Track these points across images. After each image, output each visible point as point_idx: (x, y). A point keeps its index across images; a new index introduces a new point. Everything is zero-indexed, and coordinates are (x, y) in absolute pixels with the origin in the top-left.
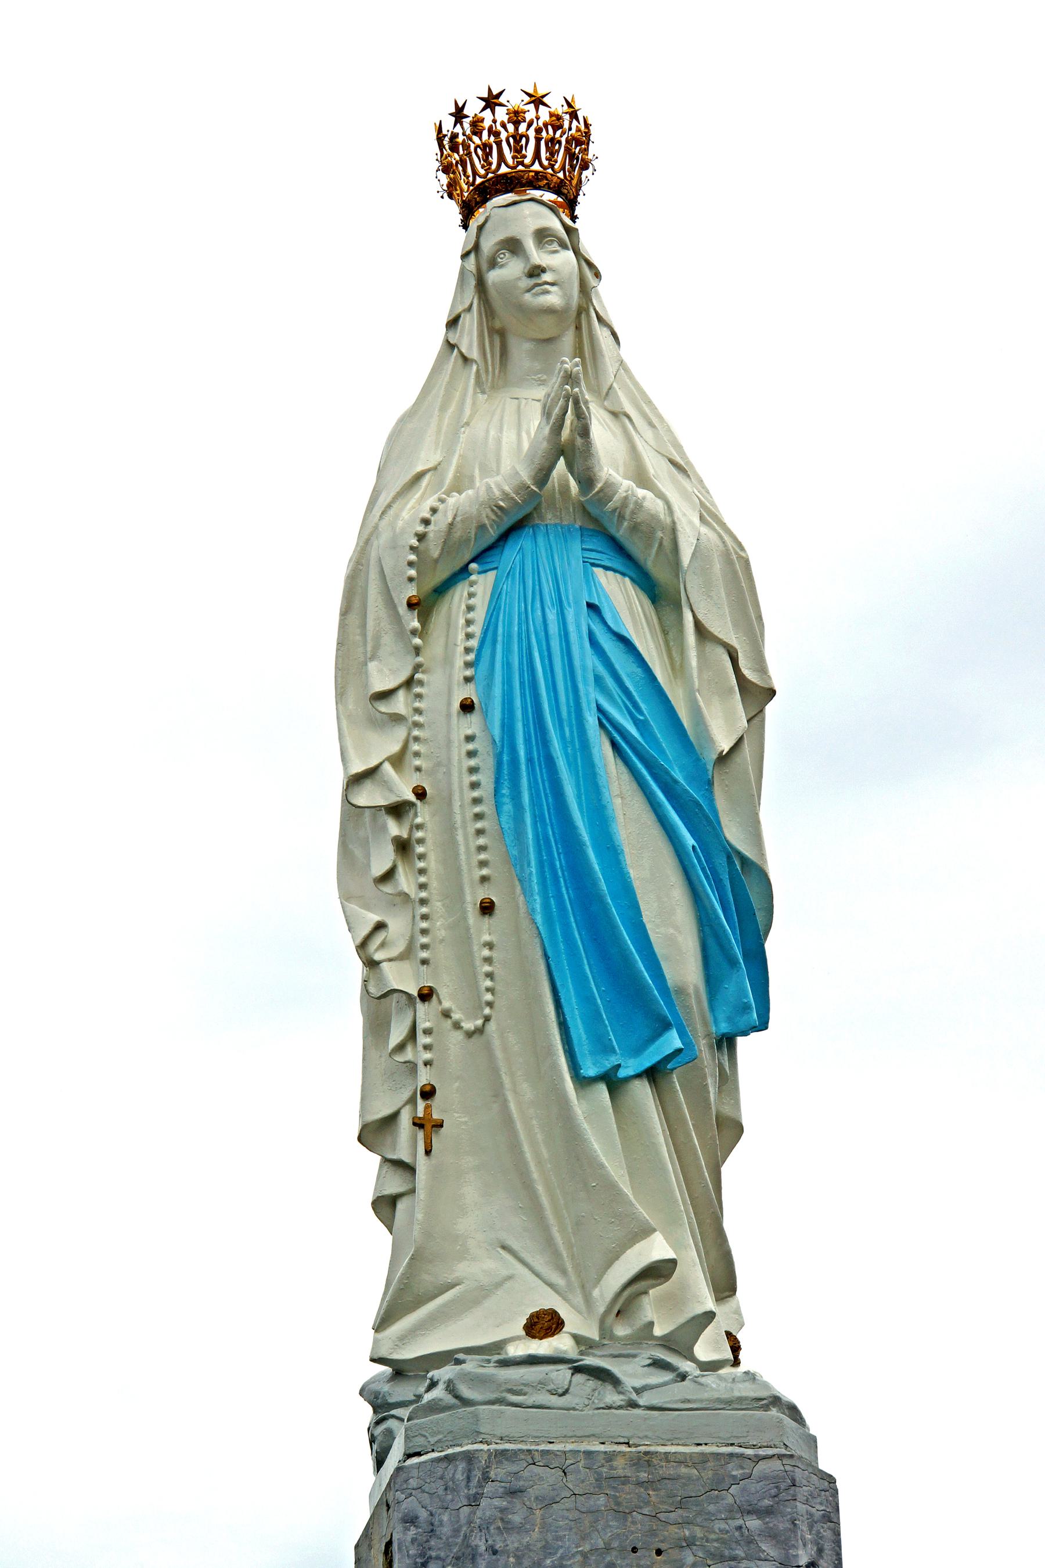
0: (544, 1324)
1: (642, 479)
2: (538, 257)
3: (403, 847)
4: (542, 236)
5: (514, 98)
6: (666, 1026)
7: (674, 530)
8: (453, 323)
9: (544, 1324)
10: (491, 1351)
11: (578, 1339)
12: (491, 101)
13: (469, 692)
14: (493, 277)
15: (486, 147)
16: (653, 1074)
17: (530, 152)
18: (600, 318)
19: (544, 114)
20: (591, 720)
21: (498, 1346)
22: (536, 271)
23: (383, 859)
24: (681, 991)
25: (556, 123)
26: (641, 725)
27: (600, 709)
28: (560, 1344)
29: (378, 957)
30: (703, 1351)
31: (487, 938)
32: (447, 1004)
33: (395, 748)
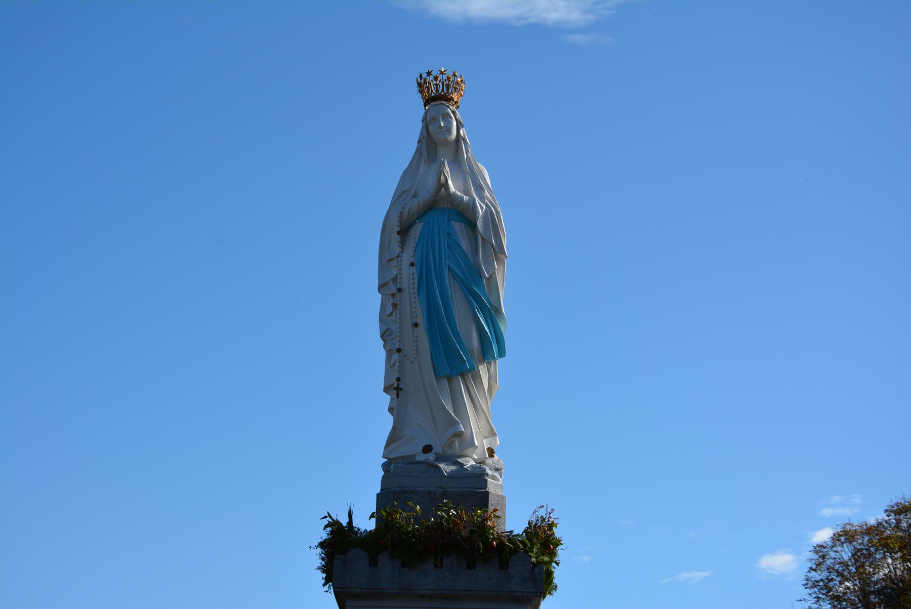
3: (395, 305)
9: (428, 449)
11: (436, 454)
12: (429, 74)
14: (430, 128)
15: (428, 87)
17: (440, 89)
19: (445, 77)
23: (390, 309)
25: (448, 79)
28: (431, 457)
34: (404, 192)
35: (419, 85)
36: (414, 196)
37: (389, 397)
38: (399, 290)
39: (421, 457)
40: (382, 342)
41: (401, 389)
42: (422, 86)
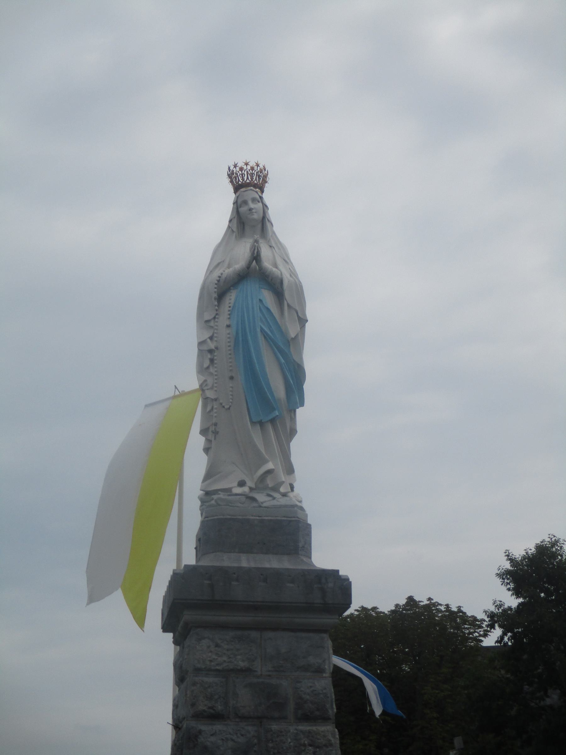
0: (242, 484)
1: (276, 267)
2: (252, 205)
3: (212, 361)
4: (254, 200)
8: (230, 221)
10: (228, 491)
13: (228, 323)
16: (273, 421)
18: (268, 220)
20: (258, 330)
22: (250, 210)
23: (207, 363)
26: (272, 332)
27: (261, 327)
28: (246, 489)
30: (282, 490)
31: (231, 385)
32: (221, 401)
42: (231, 175)
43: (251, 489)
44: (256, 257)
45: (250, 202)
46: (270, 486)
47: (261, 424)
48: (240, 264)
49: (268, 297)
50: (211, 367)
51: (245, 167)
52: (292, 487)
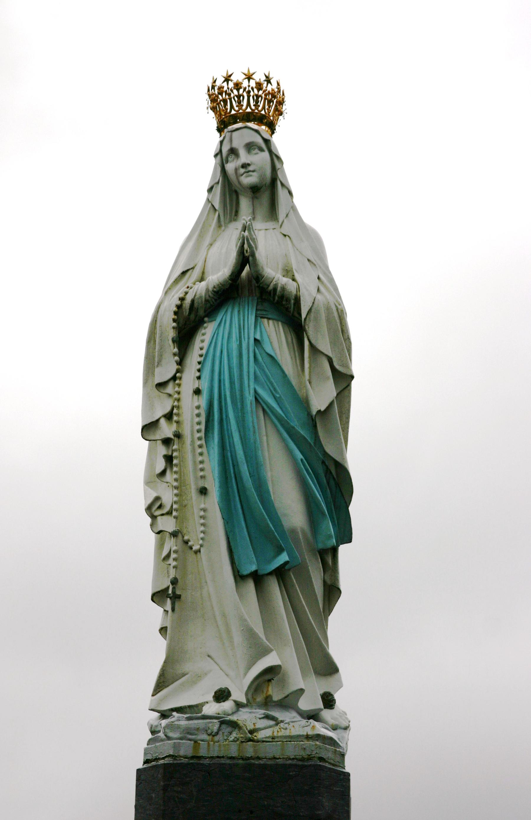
0: (222, 695)
1: (288, 272)
3: (169, 459)
5: (238, 77)
6: (280, 550)
7: (297, 300)
8: (210, 190)
9: (222, 695)
12: (227, 79)
15: (225, 101)
18: (282, 185)
19: (253, 83)
20: (250, 398)
21: (197, 708)
23: (161, 464)
24: (293, 531)
25: (259, 86)
28: (227, 705)
29: (157, 513)
30: (304, 704)
31: (202, 506)
33: (168, 409)
34: (188, 270)
35: (213, 99)
36: (202, 279)
37: (159, 610)
38: (178, 435)
39: (212, 708)
40: (149, 520)
41: (179, 597)
42: (217, 99)
43: (239, 705)
44: (245, 257)
45: (242, 152)
46: (276, 698)
47: (258, 578)
48: (219, 272)
49: (275, 335)
50: (168, 472)
51: (245, 84)
52: (328, 701)
